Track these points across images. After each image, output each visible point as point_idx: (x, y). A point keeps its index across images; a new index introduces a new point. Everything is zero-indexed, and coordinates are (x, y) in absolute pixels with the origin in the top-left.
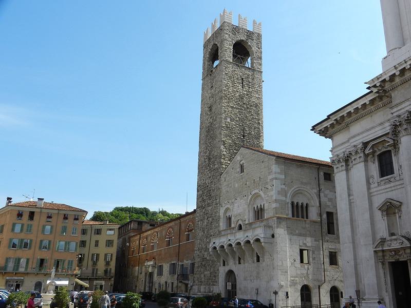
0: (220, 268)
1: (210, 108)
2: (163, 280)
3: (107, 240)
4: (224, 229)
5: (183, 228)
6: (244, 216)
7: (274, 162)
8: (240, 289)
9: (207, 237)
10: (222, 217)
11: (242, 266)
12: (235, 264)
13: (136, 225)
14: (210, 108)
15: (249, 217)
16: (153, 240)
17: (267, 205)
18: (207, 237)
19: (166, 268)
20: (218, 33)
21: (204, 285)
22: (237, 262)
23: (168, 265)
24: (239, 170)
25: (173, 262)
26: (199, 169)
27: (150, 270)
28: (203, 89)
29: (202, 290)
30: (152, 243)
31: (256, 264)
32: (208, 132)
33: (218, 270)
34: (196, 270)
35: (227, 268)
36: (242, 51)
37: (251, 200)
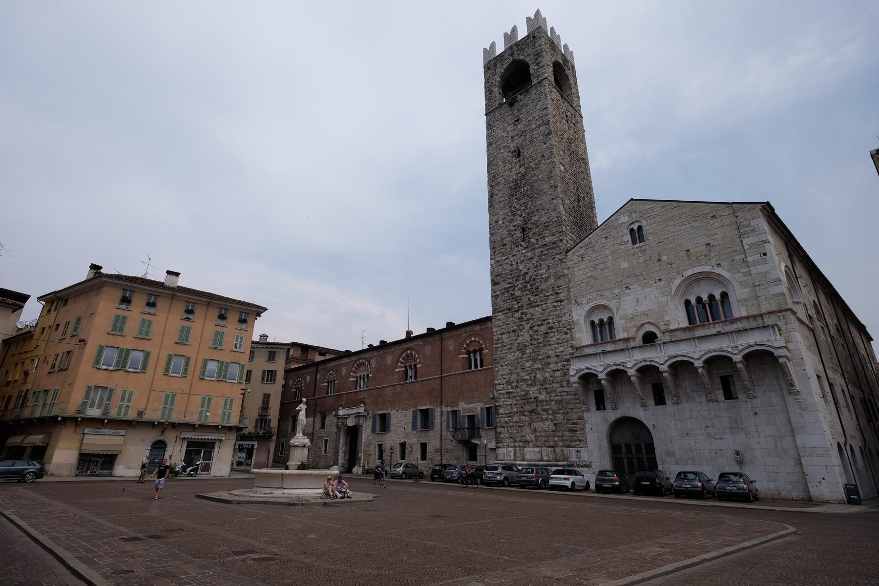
0: (586, 415)
1: (518, 153)
2: (392, 440)
3: (264, 371)
4: (589, 343)
5: (451, 348)
6: (663, 317)
7: (760, 213)
8: (669, 454)
9: (534, 360)
10: (582, 321)
11: (670, 407)
12: (644, 406)
13: (299, 352)
14: (518, 153)
15: (679, 319)
16: (354, 372)
17: (747, 290)
18: (534, 360)
19: (401, 421)
20: (515, 46)
21: (534, 446)
22: (651, 402)
23: (410, 413)
24: (628, 238)
25: (420, 408)
26: (493, 248)
27: (351, 422)
28: (490, 126)
29: (527, 457)
30: (353, 377)
31: (725, 404)
32: (516, 186)
33: (581, 418)
34: (501, 420)
35: (612, 415)
36: (563, 74)
37: (679, 286)
